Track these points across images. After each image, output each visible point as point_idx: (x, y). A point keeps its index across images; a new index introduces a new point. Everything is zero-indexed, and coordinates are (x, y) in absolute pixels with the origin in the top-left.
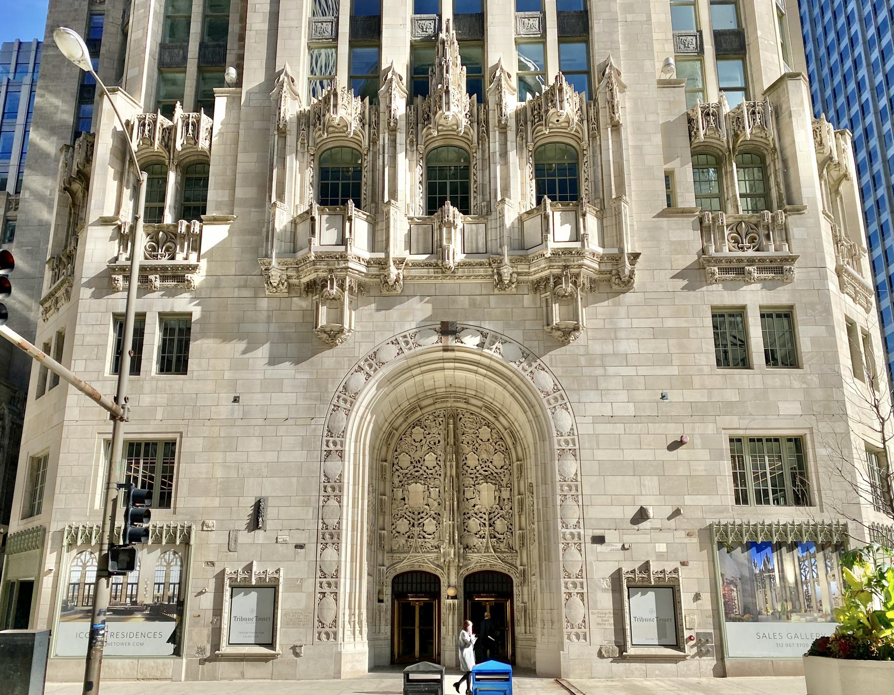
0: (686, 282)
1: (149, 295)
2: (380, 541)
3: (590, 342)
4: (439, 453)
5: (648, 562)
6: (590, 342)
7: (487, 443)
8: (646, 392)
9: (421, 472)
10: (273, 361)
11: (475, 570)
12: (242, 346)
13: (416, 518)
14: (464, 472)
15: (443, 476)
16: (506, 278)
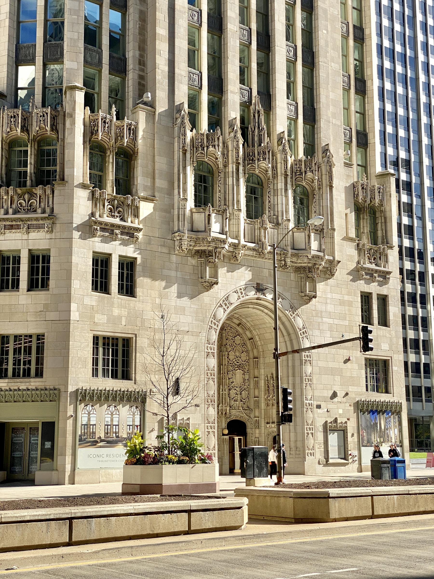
0: (352, 277)
1: (114, 243)
3: (317, 303)
5: (336, 418)
6: (317, 303)
8: (337, 333)
10: (180, 296)
12: (163, 284)
16: (289, 263)
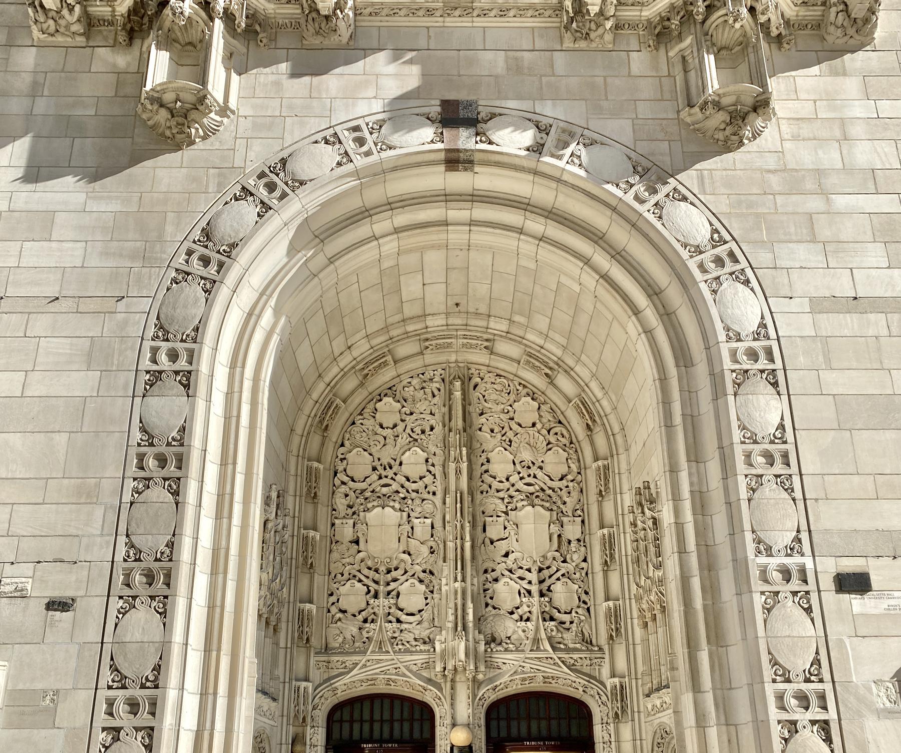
2: (292, 624)
4: (432, 449)
7: (531, 431)
9: (395, 486)
11: (513, 689)
13: (381, 579)
14: (485, 487)
15: (439, 495)
